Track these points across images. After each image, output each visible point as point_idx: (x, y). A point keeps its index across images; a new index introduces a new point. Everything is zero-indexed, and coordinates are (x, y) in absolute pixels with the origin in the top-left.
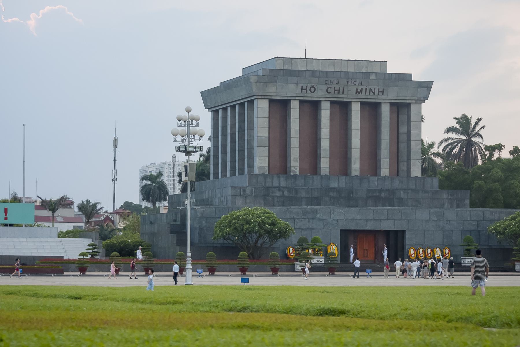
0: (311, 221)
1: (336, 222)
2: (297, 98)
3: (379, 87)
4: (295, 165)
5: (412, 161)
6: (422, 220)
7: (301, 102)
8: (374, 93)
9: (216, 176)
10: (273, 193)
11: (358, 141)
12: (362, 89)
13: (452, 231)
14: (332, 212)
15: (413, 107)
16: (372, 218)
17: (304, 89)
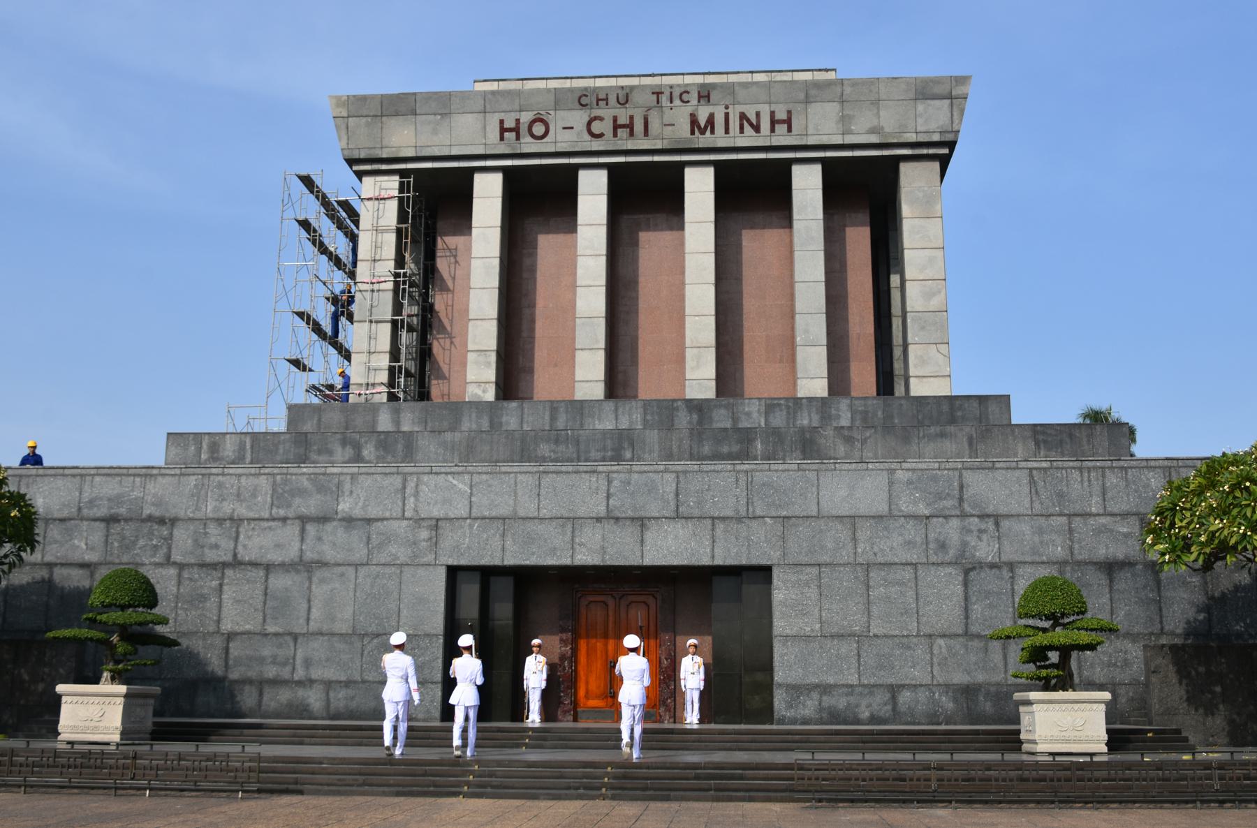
0: (311, 529)
1: (424, 534)
3: (773, 107)
6: (852, 520)
7: (510, 175)
8: (757, 129)
10: (320, 452)
12: (712, 116)
13: (1011, 566)
14: (408, 491)
16: (602, 510)
17: (510, 130)
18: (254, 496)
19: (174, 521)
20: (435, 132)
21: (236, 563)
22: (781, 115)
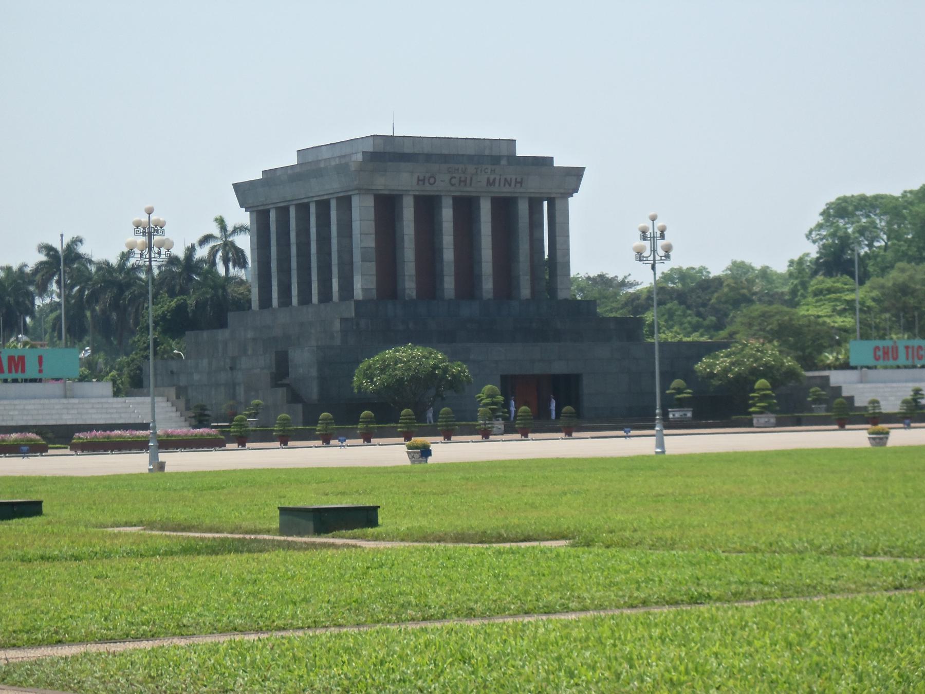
4: (410, 286)
8: (510, 185)
9: (265, 302)
15: (558, 204)
22: (519, 180)
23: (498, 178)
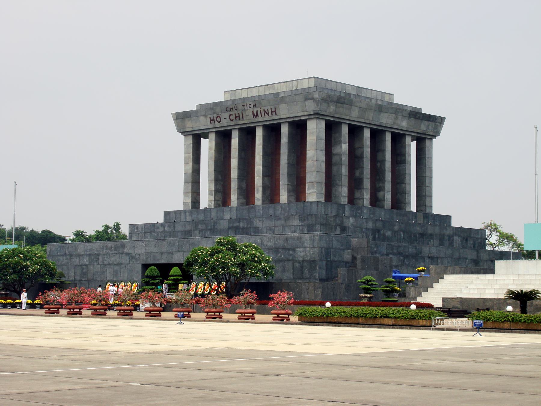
0: (120, 255)
2: (211, 130)
3: (272, 107)
5: (307, 185)
8: (268, 114)
11: (261, 167)
12: (257, 111)
18: (112, 248)
19: (98, 255)
20: (196, 123)
21: (109, 264)
22: (273, 110)
23: (259, 110)
